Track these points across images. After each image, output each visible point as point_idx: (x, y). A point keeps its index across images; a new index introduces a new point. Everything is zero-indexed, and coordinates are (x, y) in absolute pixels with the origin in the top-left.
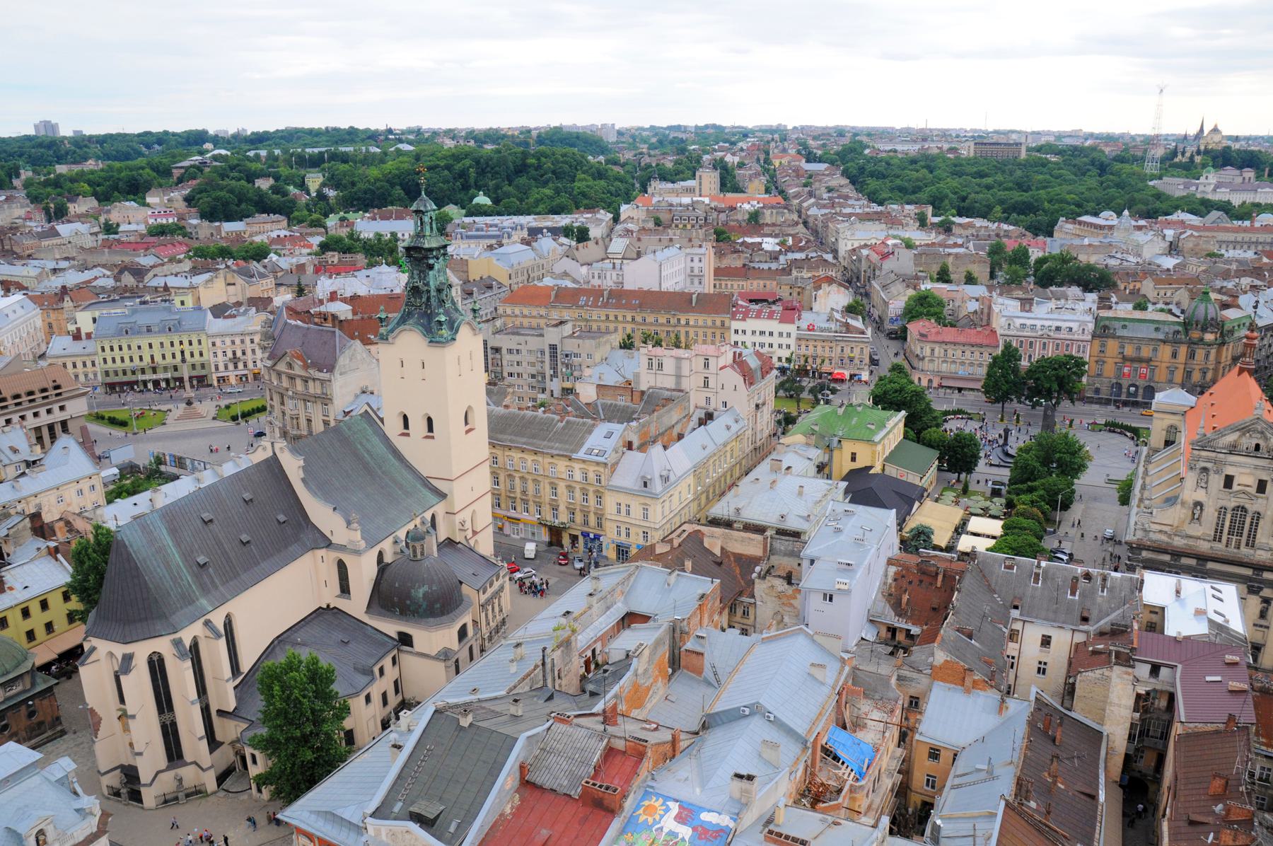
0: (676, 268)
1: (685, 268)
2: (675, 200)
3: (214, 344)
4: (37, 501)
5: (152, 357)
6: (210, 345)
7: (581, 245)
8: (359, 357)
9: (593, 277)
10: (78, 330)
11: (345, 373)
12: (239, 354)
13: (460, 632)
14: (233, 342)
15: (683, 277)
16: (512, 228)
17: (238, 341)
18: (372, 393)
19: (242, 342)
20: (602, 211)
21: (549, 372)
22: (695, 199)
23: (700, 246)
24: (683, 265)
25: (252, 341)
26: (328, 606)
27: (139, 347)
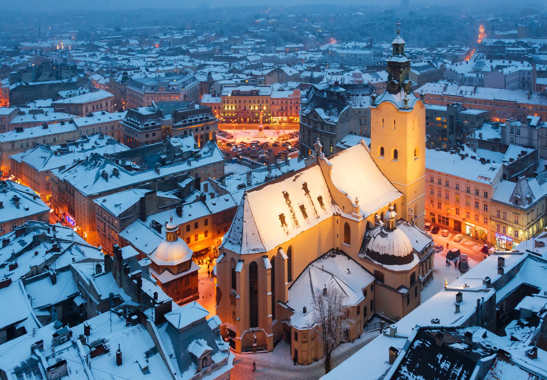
0: (514, 78)
1: (519, 78)
2: (507, 41)
3: (273, 103)
4: (196, 172)
5: (245, 107)
6: (271, 103)
7: (458, 63)
8: (350, 114)
9: (465, 81)
10: (215, 92)
11: (343, 122)
12: (284, 108)
13: (411, 277)
14: (282, 102)
15: (518, 82)
16: (416, 54)
17: (284, 102)
18: (355, 134)
19: (286, 102)
20: (464, 46)
21: (449, 131)
22: (518, 40)
23: (528, 66)
24: (518, 76)
25: (291, 103)
26: (338, 248)
27: (240, 101)
